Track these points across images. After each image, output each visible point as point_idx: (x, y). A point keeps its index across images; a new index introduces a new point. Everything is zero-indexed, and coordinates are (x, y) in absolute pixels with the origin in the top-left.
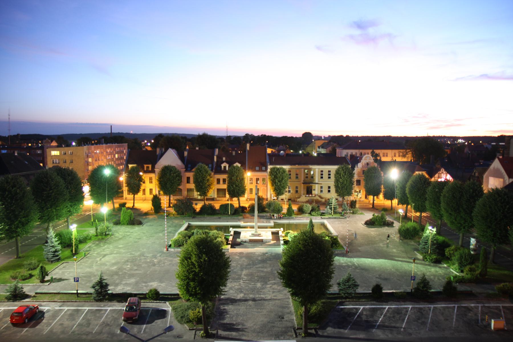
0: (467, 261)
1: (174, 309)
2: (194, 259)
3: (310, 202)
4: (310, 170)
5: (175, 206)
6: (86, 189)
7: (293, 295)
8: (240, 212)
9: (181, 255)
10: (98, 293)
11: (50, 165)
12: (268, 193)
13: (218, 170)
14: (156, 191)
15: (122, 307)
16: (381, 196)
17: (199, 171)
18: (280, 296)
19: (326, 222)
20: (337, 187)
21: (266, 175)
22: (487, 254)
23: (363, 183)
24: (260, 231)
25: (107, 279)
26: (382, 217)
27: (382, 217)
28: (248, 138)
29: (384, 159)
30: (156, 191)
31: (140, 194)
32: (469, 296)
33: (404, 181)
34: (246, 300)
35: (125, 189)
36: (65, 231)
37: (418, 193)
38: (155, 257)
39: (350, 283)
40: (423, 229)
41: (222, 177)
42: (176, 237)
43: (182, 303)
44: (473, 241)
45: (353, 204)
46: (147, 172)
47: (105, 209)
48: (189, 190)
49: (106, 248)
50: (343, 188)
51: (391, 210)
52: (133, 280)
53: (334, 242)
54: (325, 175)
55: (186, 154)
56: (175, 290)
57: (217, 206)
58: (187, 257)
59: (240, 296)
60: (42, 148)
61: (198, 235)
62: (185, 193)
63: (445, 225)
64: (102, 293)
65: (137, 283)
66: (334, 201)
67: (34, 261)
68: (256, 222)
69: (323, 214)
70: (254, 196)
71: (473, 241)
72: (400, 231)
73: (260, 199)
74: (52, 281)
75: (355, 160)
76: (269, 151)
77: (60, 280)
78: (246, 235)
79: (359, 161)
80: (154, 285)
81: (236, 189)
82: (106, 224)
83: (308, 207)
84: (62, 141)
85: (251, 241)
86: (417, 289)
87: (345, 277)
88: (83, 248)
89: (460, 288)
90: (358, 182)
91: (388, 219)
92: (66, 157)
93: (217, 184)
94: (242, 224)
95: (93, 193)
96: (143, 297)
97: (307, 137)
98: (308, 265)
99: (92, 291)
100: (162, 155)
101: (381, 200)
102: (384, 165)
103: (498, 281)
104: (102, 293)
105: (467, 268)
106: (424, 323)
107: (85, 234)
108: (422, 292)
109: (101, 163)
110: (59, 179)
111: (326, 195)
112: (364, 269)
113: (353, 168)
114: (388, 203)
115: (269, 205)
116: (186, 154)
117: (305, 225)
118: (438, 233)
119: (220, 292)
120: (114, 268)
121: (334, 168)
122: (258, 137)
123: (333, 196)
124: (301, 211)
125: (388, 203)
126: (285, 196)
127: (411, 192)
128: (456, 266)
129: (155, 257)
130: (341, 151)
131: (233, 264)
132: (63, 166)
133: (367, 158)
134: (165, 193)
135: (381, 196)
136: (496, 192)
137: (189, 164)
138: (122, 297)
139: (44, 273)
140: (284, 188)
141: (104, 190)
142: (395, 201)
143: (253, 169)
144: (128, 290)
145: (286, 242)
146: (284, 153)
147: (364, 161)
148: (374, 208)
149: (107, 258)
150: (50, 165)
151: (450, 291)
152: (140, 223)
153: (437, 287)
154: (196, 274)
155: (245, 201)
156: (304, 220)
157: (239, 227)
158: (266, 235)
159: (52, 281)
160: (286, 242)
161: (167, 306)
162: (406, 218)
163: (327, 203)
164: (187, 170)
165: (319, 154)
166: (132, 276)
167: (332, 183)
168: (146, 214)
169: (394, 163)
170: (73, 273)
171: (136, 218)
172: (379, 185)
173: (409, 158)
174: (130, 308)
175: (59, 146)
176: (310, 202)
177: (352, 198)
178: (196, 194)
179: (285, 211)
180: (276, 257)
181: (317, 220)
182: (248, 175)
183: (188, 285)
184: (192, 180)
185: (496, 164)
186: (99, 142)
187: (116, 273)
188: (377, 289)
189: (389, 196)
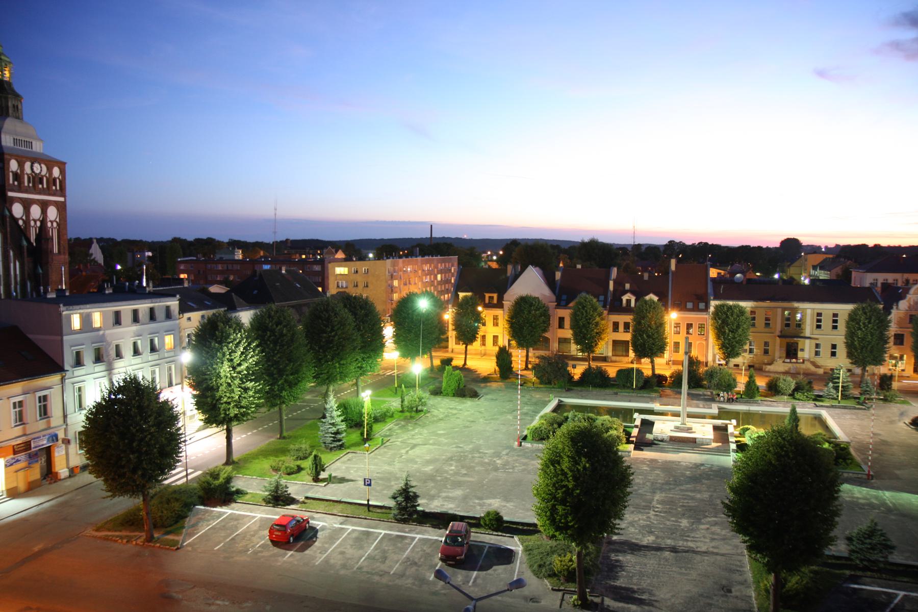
1: (528, 550)
2: (566, 464)
4: (794, 311)
5: (536, 368)
6: (389, 331)
7: (751, 548)
8: (654, 385)
9: (545, 456)
10: (402, 509)
11: (332, 290)
12: (710, 352)
13: (616, 307)
14: (503, 341)
15: (438, 536)
17: (582, 306)
18: (725, 549)
19: (824, 413)
21: (706, 318)
23: (909, 341)
24: (690, 422)
25: (417, 487)
28: (673, 248)
30: (503, 341)
31: (477, 344)
34: (659, 549)
35: (452, 334)
36: (352, 400)
38: (498, 455)
41: (623, 319)
42: (536, 422)
45: (885, 382)
46: (488, 306)
47: (418, 367)
48: (563, 341)
49: (418, 433)
50: (865, 347)
52: (458, 493)
53: (842, 453)
54: (827, 322)
55: (558, 275)
57: (612, 372)
58: (553, 461)
59: (649, 540)
60: (322, 262)
61: (575, 422)
62: (555, 346)
64: (407, 508)
65: (465, 498)
67: (305, 445)
68: (683, 405)
69: (818, 398)
70: (681, 356)
73: (693, 363)
74: (330, 480)
75: (893, 295)
76: (713, 273)
77: (342, 480)
78: (663, 427)
79: (902, 297)
80: (495, 504)
81: (649, 343)
82: (419, 392)
84: (354, 250)
85: (673, 440)
87: (864, 526)
88: (380, 430)
90: (899, 340)
92: (359, 278)
93: (614, 332)
94: (657, 406)
95: (399, 338)
96: (475, 522)
97: (791, 247)
99: (391, 503)
100: (516, 277)
104: (407, 508)
107: (384, 407)
109: (414, 289)
110: (346, 314)
111: (827, 362)
115: (711, 374)
116: (558, 275)
117: (781, 417)
119: (612, 529)
120: (429, 469)
121: (845, 309)
122: (754, 248)
123: (841, 363)
124: (773, 389)
126: (742, 359)
129: (498, 455)
131: (637, 480)
132: (354, 292)
134: (521, 345)
137: (564, 293)
138: (439, 520)
139: (318, 467)
140: (741, 343)
141: (418, 334)
143: (681, 306)
144: (450, 507)
145: (741, 447)
149: (417, 451)
150: (332, 290)
152: (475, 395)
154: (568, 492)
155: (664, 365)
156: (780, 407)
158: (703, 430)
159: (330, 480)
160: (741, 447)
161: (515, 544)
163: (830, 377)
164: (559, 305)
165: (814, 281)
166: (457, 485)
167: (840, 338)
168: (486, 379)
170: (364, 472)
171: (468, 386)
174: (452, 538)
175: (348, 259)
177: (883, 370)
178: (574, 349)
179: (741, 387)
180: (721, 473)
181: (805, 409)
182: (673, 316)
183: (553, 510)
184: (567, 323)
186: (410, 254)
187: (431, 478)
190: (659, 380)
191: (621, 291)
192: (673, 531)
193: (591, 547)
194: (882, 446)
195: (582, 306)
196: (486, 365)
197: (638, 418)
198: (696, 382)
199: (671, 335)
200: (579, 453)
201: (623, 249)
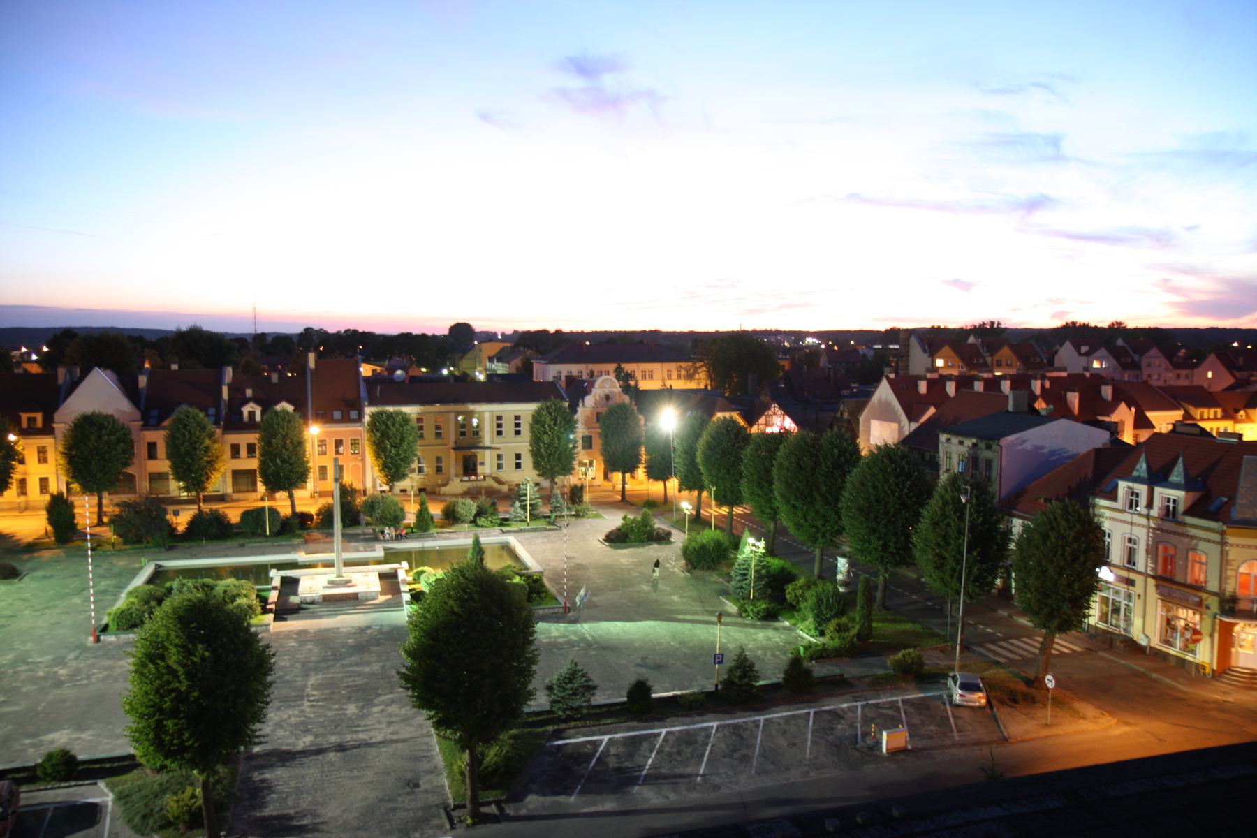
0: (833, 608)
1: (122, 798)
2: (173, 658)
3: (472, 494)
4: (469, 415)
5: (116, 522)
7: (438, 725)
8: (296, 527)
9: (138, 651)
12: (368, 476)
13: (234, 423)
14: (58, 484)
16: (641, 472)
17: (182, 425)
18: (407, 732)
19: (513, 540)
20: (536, 454)
21: (360, 431)
22: (870, 589)
23: (597, 443)
24: (350, 573)
26: (645, 522)
27: (645, 522)
28: (311, 338)
29: (644, 385)
30: (58, 484)
32: (838, 685)
33: (693, 434)
34: (320, 751)
37: (724, 462)
39: (576, 683)
40: (736, 545)
42: (122, 602)
43: (146, 777)
44: (842, 564)
45: (575, 494)
48: (157, 477)
51: (663, 505)
53: (535, 587)
54: (508, 428)
55: (143, 381)
56: (124, 746)
57: (234, 515)
58: (153, 655)
59: (305, 741)
61: (183, 594)
62: (143, 485)
63: (782, 531)
66: (530, 490)
68: (337, 550)
69: (504, 522)
70: (330, 485)
71: (842, 564)
72: (686, 552)
73: (346, 492)
75: (578, 389)
76: (366, 370)
78: (312, 584)
79: (587, 392)
80: (60, 739)
81: (284, 470)
83: (469, 507)
85: (327, 600)
86: (728, 684)
87: (564, 670)
90: (588, 443)
91: (659, 524)
94: (301, 557)
97: (462, 335)
98: (473, 649)
100: (73, 385)
101: (640, 483)
102: (645, 400)
103: (894, 648)
105: (831, 626)
106: (745, 759)
108: (739, 689)
111: (511, 476)
112: (606, 647)
113: (574, 408)
114: (656, 488)
115: (371, 506)
116: (143, 381)
117: (461, 551)
118: (770, 551)
119: (250, 740)
121: (527, 409)
123: (527, 477)
124: (451, 517)
125: (656, 488)
126: (410, 482)
127: (707, 459)
129: (61, 661)
130: (546, 367)
131: (281, 662)
133: (606, 384)
134: (87, 489)
135: (641, 472)
136: (885, 453)
137: (152, 408)
140: (407, 461)
142: (673, 483)
143: (325, 417)
145: (417, 596)
146: (403, 376)
147: (598, 391)
148: (625, 501)
151: (800, 682)
153: (770, 674)
154: (181, 698)
155: (307, 499)
156: (459, 539)
157: (294, 565)
158: (366, 581)
160: (417, 596)
161: (102, 794)
162: (698, 521)
163: (515, 494)
165: (491, 376)
167: (523, 445)
168: (32, 547)
169: (667, 393)
172: (635, 446)
173: (701, 381)
176: (472, 494)
177: (572, 480)
178: (175, 487)
179: (410, 519)
180: (393, 634)
181: (491, 537)
182: (314, 431)
183: (159, 728)
184: (161, 450)
185: (884, 392)
188: (640, 690)
189: (659, 471)
190: (302, 520)
191: (238, 400)
192: (336, 724)
193: (222, 770)
194: (576, 574)
195: (182, 425)
196: (33, 526)
197: (276, 576)
198: (351, 517)
199: (314, 457)
200: (192, 638)
201: (240, 342)
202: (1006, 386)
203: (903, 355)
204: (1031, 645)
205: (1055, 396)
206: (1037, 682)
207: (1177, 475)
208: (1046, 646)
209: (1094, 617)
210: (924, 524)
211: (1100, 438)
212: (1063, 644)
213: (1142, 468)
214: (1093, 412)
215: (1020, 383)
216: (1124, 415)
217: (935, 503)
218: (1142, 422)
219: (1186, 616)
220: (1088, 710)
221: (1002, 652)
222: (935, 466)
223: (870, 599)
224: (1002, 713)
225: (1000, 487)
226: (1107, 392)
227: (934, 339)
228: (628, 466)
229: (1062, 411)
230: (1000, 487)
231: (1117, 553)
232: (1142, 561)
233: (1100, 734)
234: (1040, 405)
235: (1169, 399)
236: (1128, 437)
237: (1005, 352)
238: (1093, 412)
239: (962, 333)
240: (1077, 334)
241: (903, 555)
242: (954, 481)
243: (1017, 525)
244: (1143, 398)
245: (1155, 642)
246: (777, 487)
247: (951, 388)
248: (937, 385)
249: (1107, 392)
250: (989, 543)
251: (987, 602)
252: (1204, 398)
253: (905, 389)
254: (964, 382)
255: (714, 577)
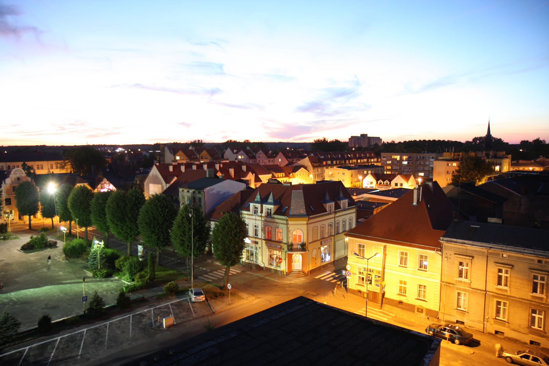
0: (137, 268)
22: (153, 258)
23: (14, 202)
27: (43, 238)
29: (38, 172)
32: (142, 302)
33: (64, 195)
40: (90, 245)
44: (140, 248)
51: (52, 229)
63: (112, 236)
71: (140, 248)
72: (65, 251)
79: (7, 176)
86: (90, 310)
89: (133, 297)
90: (8, 202)
91: (50, 239)
101: (39, 219)
102: (39, 179)
103: (165, 282)
105: (137, 276)
106: (101, 343)
108: (96, 311)
114: (48, 221)
118: (107, 246)
125: (48, 221)
127: (73, 205)
128: (127, 275)
133: (18, 172)
135: (39, 215)
136: (156, 198)
142: (56, 219)
148: (31, 229)
151: (125, 303)
153: (110, 302)
162: (70, 235)
172: (36, 201)
173: (68, 169)
185: (154, 171)
188: (45, 321)
189: (49, 213)
202: (205, 167)
203: (162, 155)
204: (221, 273)
205: (225, 170)
206: (224, 288)
207: (271, 200)
208: (227, 272)
209: (244, 258)
210: (175, 227)
211: (243, 186)
212: (233, 270)
213: (258, 197)
214: (239, 177)
215: (211, 165)
216: (251, 177)
217: (178, 218)
218: (257, 180)
219: (276, 253)
220: (244, 295)
221: (210, 277)
222: (178, 202)
223: (153, 262)
224: (212, 302)
225: (205, 209)
226: (244, 168)
227: (175, 148)
228: (32, 212)
229: (227, 176)
230: (205, 209)
231: (251, 233)
232: (260, 234)
233: (250, 304)
234: (219, 174)
235: (267, 170)
236: (253, 186)
237: (204, 153)
238: (239, 177)
239: (187, 145)
240: (232, 145)
241: (167, 241)
242: (186, 208)
243: (213, 224)
244: (257, 170)
245: (267, 265)
246: (108, 216)
247: (183, 169)
248: (177, 167)
249: (244, 168)
250: (202, 233)
251: (203, 257)
252: (278, 169)
253: (163, 170)
254: (188, 166)
255: (80, 261)
